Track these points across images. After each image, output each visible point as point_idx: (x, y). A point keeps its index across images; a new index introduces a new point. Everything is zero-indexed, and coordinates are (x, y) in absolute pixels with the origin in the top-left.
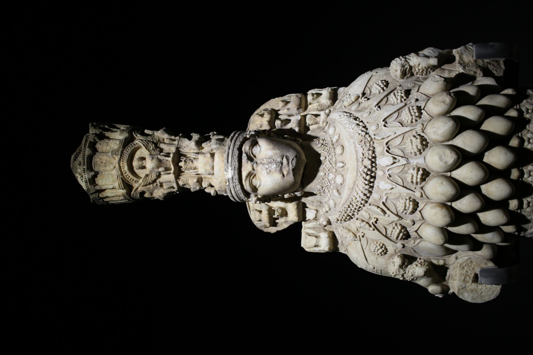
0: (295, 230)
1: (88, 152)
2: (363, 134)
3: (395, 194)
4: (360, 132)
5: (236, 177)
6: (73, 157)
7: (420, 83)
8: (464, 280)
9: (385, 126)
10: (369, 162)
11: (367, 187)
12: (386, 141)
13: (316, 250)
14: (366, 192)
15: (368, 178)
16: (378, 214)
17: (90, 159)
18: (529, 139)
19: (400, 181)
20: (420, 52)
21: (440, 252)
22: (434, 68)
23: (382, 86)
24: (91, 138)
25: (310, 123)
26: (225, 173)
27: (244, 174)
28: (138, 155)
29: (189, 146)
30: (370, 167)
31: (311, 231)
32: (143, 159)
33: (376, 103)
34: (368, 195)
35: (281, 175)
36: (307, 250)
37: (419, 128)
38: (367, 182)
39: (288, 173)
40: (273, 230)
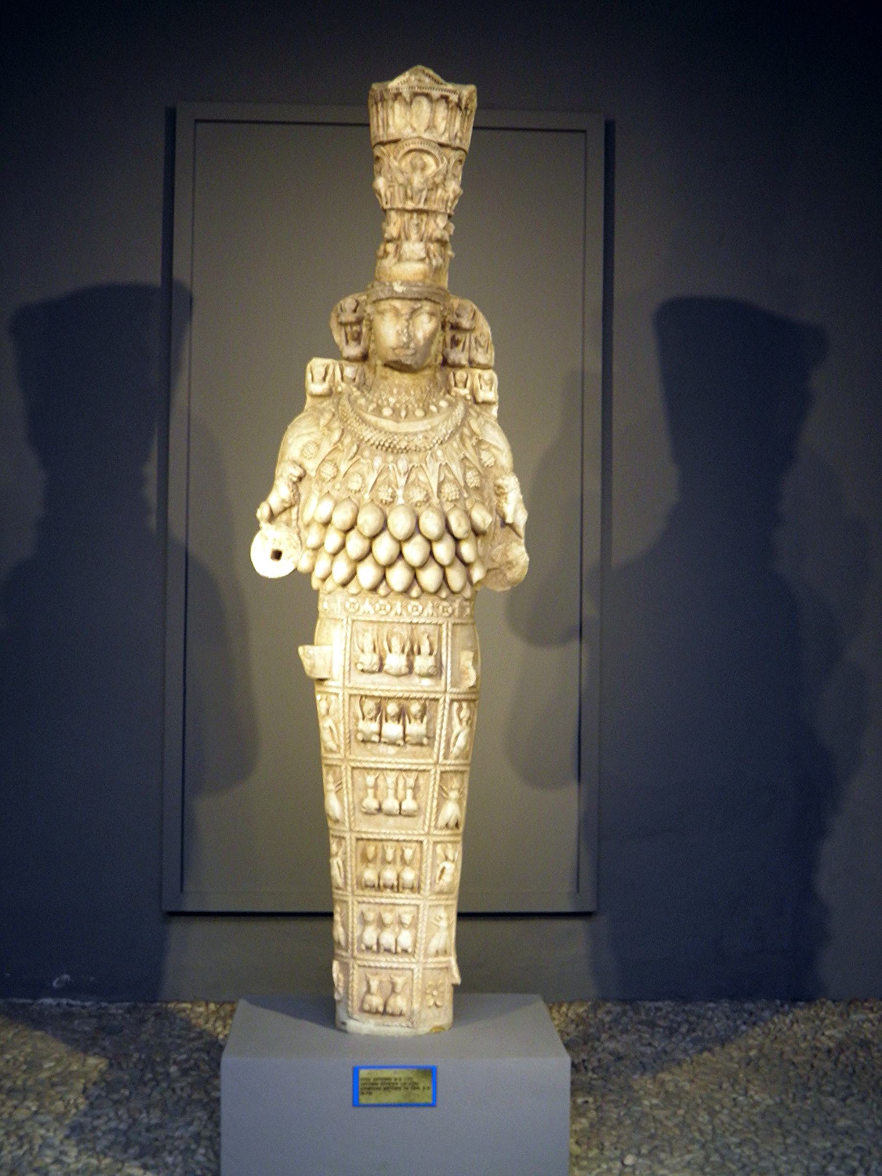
0: (334, 353)
1: (436, 94)
2: (434, 441)
3: (368, 473)
4: (437, 438)
5: (394, 295)
6: (431, 72)
7: (487, 503)
8: (275, 540)
9: (441, 465)
10: (403, 447)
11: (377, 443)
12: (424, 465)
13: (309, 376)
14: (372, 442)
15: (387, 445)
16: (348, 454)
17: (427, 96)
18: (417, 607)
19: (382, 478)
20: (521, 506)
21: (307, 517)
22: (503, 519)
23: (488, 463)
24: (454, 98)
25: (458, 377)
26: (400, 282)
27: (397, 304)
28: (429, 160)
29: (439, 226)
30: (398, 447)
31: (330, 371)
32: (424, 168)
33: (468, 455)
34: (369, 444)
35: (395, 346)
36: (308, 366)
37: (435, 500)
38: (382, 443)
39: (397, 355)
40: (334, 325)
